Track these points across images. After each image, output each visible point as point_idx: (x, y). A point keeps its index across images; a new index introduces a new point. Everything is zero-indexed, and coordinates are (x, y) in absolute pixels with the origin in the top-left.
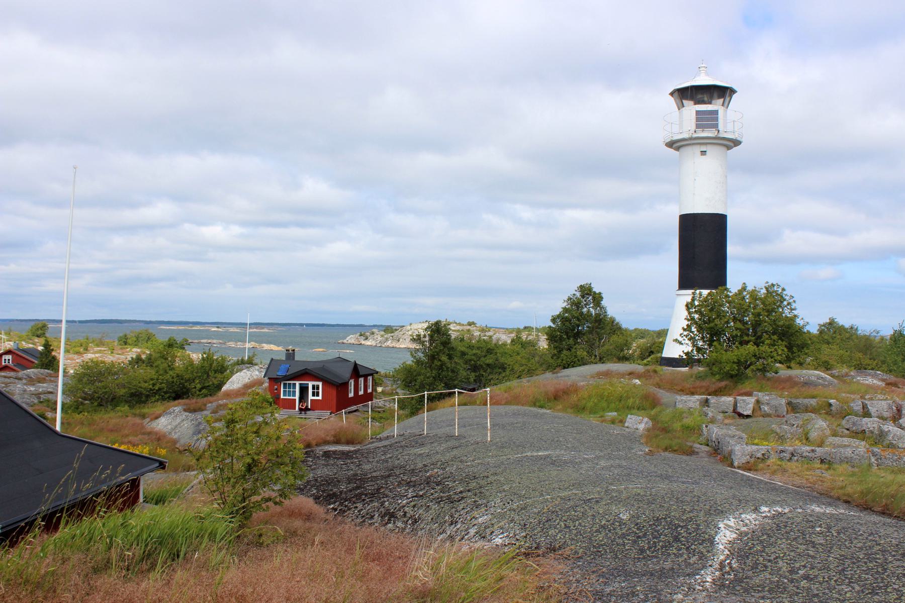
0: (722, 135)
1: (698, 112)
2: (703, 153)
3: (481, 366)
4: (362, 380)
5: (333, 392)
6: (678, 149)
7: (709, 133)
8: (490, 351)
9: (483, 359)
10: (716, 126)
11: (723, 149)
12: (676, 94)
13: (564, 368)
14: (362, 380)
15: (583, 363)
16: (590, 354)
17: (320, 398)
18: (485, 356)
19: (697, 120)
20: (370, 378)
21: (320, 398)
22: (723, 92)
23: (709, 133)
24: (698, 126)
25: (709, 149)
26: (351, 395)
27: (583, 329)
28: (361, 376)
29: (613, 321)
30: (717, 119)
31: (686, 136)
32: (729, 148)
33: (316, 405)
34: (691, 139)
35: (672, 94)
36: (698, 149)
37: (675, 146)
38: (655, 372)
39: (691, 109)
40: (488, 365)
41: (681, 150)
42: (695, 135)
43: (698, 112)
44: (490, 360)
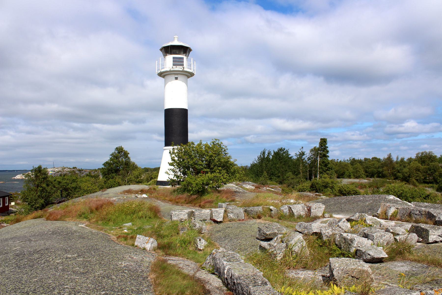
0: (185, 70)
1: (174, 58)
2: (176, 78)
3: (69, 188)
7: (179, 68)
9: (70, 185)
10: (183, 65)
11: (186, 77)
15: (120, 185)
16: (123, 180)
18: (71, 183)
19: (174, 61)
22: (185, 50)
23: (179, 68)
24: (174, 65)
25: (179, 77)
27: (119, 168)
29: (134, 164)
30: (183, 62)
34: (170, 71)
36: (173, 77)
38: (154, 189)
42: (172, 69)
43: (174, 58)
44: (74, 185)
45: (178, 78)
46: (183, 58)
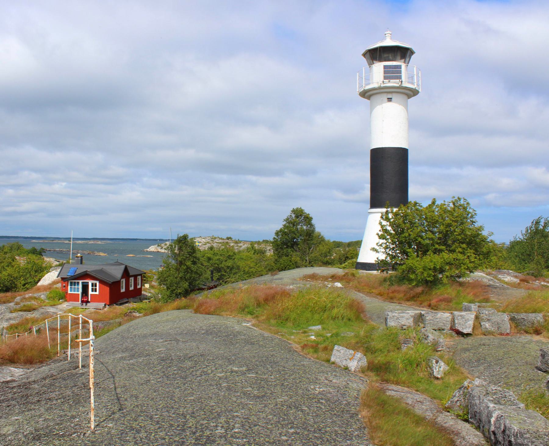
1: (385, 67)
2: (390, 100)
4: (132, 280)
5: (107, 289)
6: (369, 98)
7: (394, 83)
8: (229, 257)
9: (224, 263)
10: (400, 78)
11: (406, 97)
12: (368, 53)
13: (282, 270)
14: (132, 280)
17: (97, 293)
19: (385, 72)
20: (139, 278)
21: (97, 293)
23: (394, 83)
24: (385, 78)
25: (394, 97)
26: (123, 290)
28: (132, 276)
31: (375, 85)
32: (409, 97)
33: (95, 299)
34: (380, 88)
35: (364, 55)
36: (385, 97)
37: (367, 94)
39: (379, 67)
40: (228, 267)
41: (372, 98)
42: (382, 85)
43: (385, 67)
44: (230, 263)
45: (393, 99)
46: (400, 67)
